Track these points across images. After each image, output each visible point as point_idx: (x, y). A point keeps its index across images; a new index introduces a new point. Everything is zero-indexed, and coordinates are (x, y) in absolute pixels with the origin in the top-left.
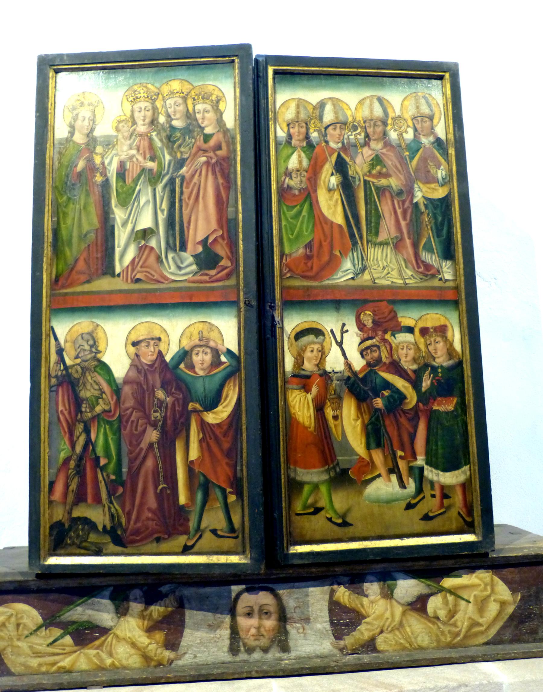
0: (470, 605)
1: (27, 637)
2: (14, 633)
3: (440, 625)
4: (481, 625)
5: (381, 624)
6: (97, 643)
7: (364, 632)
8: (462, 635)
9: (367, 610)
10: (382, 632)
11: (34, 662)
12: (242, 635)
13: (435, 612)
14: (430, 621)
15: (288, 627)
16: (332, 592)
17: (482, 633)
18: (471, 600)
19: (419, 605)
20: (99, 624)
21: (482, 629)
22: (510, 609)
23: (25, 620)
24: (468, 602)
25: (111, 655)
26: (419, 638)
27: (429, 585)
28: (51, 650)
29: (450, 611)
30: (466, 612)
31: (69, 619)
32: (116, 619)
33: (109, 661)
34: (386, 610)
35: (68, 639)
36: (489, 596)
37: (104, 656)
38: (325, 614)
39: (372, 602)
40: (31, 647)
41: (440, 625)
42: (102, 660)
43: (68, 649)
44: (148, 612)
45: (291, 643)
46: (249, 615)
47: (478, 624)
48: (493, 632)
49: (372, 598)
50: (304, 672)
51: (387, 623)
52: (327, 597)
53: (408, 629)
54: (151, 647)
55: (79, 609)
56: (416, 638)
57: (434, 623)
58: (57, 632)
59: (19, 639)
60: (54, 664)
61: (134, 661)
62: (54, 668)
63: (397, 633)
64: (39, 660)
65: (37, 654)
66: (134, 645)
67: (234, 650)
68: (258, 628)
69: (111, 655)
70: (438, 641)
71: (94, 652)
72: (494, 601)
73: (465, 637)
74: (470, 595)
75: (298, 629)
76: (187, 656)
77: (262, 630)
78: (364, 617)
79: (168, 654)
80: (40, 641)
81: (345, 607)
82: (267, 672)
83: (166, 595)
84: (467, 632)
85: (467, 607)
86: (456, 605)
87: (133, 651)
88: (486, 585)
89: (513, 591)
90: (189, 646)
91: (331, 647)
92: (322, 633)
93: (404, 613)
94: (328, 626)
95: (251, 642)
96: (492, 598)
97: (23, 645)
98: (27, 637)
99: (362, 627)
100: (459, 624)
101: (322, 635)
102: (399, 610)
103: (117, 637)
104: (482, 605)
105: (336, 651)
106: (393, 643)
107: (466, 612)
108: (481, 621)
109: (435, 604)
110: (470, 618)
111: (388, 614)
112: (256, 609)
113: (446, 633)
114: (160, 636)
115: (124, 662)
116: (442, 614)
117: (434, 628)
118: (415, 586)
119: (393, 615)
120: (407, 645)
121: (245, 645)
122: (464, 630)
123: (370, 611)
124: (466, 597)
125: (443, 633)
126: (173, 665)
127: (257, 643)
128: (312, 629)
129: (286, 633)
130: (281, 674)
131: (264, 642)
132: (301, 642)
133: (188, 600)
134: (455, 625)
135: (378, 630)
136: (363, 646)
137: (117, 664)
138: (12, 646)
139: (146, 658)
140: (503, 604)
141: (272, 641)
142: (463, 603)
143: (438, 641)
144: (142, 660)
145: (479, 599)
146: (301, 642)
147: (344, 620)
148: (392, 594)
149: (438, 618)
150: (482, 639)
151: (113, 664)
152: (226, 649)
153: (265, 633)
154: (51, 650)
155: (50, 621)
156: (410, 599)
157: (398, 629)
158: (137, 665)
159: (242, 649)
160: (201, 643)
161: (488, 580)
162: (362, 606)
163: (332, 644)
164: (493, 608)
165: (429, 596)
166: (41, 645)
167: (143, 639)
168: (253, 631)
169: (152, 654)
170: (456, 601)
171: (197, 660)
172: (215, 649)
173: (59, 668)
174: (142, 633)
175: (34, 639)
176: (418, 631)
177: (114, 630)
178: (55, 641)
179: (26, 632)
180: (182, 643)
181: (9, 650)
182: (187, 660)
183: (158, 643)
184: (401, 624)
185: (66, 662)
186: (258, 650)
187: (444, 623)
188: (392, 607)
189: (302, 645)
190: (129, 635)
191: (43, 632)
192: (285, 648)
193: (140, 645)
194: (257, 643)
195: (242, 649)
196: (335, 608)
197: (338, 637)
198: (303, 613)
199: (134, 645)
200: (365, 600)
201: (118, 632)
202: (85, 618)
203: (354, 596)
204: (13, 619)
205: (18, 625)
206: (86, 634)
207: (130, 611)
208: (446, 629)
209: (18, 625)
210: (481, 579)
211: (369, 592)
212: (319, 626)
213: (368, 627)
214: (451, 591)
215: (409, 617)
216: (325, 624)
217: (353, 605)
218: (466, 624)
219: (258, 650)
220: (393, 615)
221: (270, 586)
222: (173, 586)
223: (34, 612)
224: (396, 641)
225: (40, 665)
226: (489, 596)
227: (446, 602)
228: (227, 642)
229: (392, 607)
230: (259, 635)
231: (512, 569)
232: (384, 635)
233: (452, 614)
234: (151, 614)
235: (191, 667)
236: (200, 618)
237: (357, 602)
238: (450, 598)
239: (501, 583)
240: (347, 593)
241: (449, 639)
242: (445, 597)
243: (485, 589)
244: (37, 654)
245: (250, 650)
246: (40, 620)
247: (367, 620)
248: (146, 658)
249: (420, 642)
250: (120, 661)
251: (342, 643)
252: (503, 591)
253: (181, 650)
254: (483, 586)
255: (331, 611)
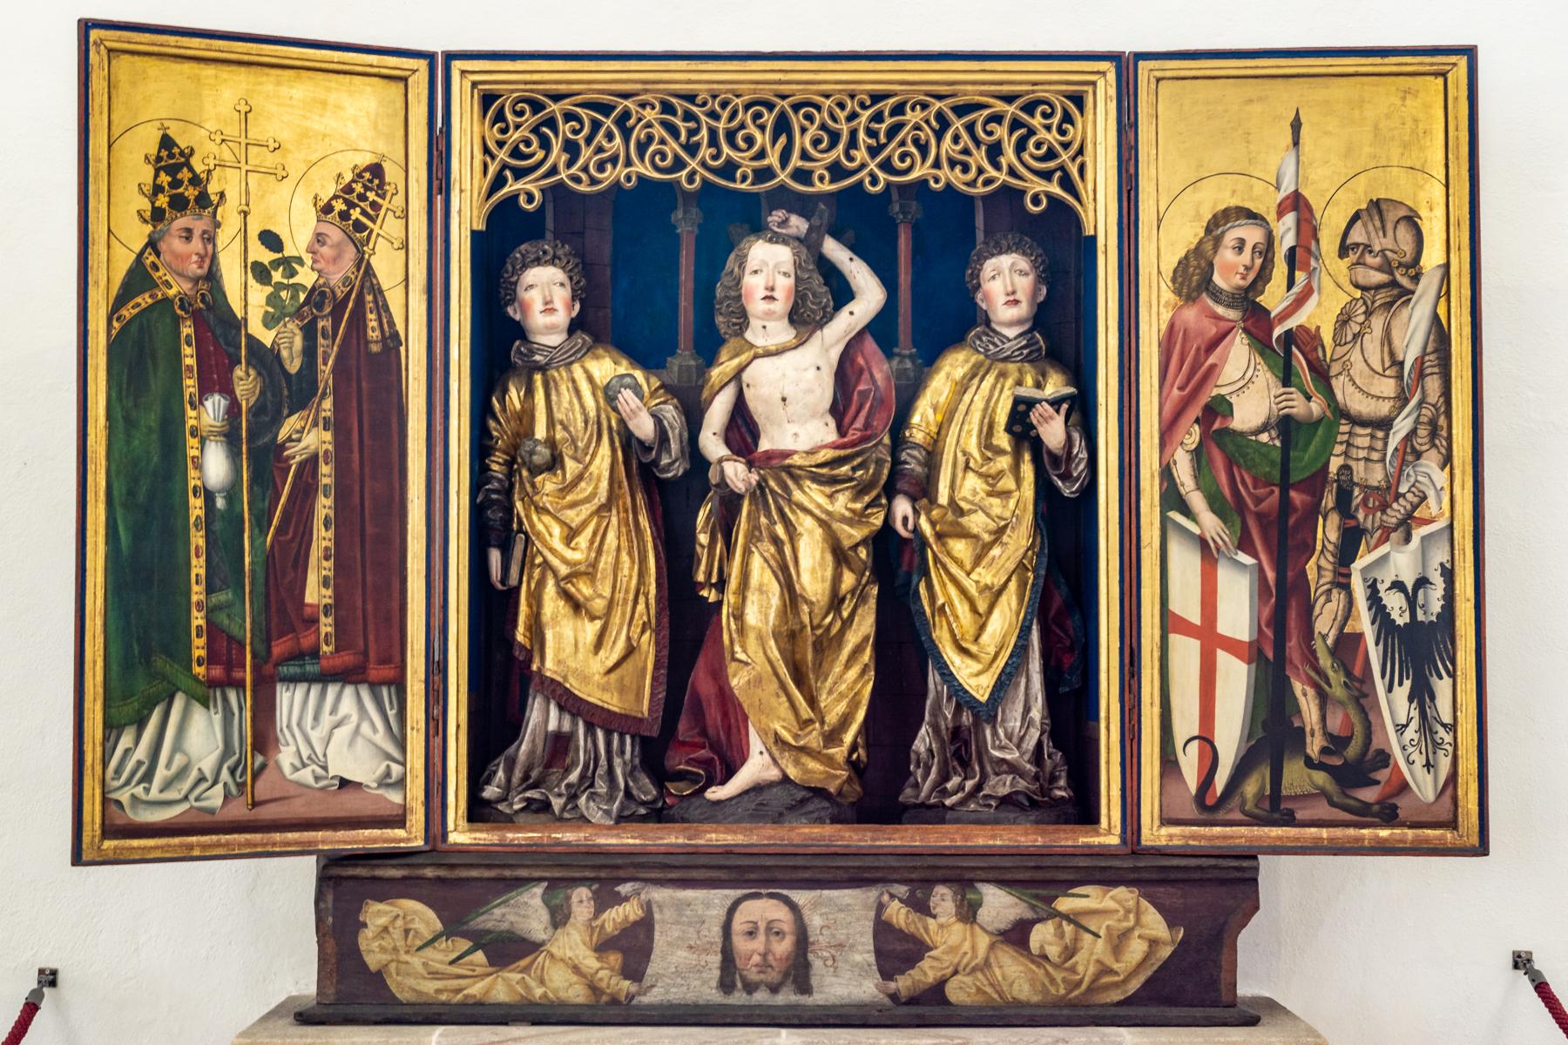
0: (1100, 941)
1: (419, 949)
2: (400, 944)
3: (1049, 968)
4: (1116, 973)
5: (956, 961)
6: (523, 963)
7: (926, 972)
8: (1084, 986)
9: (935, 938)
10: (956, 972)
11: (429, 987)
12: (738, 963)
13: (1042, 947)
14: (1033, 962)
15: (811, 957)
16: (881, 907)
17: (1116, 985)
18: (1102, 933)
19: (1016, 936)
20: (527, 936)
21: (1116, 979)
22: (1166, 952)
23: (417, 925)
24: (1097, 936)
25: (542, 982)
26: (1016, 986)
27: (1033, 907)
28: (454, 970)
29: (1066, 947)
30: (1093, 952)
31: (481, 927)
32: (550, 931)
33: (538, 992)
34: (965, 939)
35: (479, 956)
36: (1130, 930)
37: (533, 984)
38: (867, 941)
39: (941, 926)
40: (425, 964)
41: (1049, 968)
42: (527, 988)
43: (479, 970)
44: (598, 922)
45: (814, 981)
46: (751, 934)
47: (1111, 972)
48: (1135, 985)
49: (942, 920)
50: (831, 1021)
51: (965, 961)
52: (872, 914)
53: (998, 972)
54: (602, 974)
55: (497, 912)
56: (1011, 985)
57: (1039, 965)
58: (464, 945)
59: (407, 952)
60: (459, 991)
61: (576, 993)
62: (459, 997)
63: (980, 975)
64: (439, 984)
65: (435, 975)
66: (576, 969)
67: (726, 985)
68: (764, 956)
69: (542, 982)
70: (1045, 991)
71: (519, 976)
72: (1140, 937)
73: (1089, 990)
74: (1101, 926)
75: (826, 960)
76: (655, 990)
77: (770, 958)
78: (930, 949)
79: (626, 985)
80: (439, 956)
81: (901, 931)
82: (773, 1017)
83: (626, 899)
84: (1094, 981)
85: (1094, 943)
86: (1076, 939)
87: (575, 978)
88: (1128, 911)
89: (1171, 925)
90: (659, 976)
91: (875, 991)
92: (862, 968)
93: (992, 947)
94: (871, 958)
95: (753, 975)
96: (1136, 933)
97: (416, 961)
98: (419, 949)
99: (925, 964)
100: (1080, 969)
101: (862, 970)
102: (983, 942)
103: (552, 956)
104: (1119, 942)
105: (887, 1001)
106: (973, 991)
107: (1093, 952)
108: (1116, 966)
109: (1042, 936)
110: (1098, 961)
111: (967, 946)
112: (762, 926)
113: (1059, 980)
114: (615, 959)
115: (563, 995)
116: (1053, 951)
117: (1040, 972)
118: (1011, 906)
119: (974, 948)
120: (996, 996)
121: (743, 978)
122: (1087, 979)
123: (938, 939)
124: (1093, 928)
125: (1053, 981)
126: (634, 1002)
127: (762, 976)
128: (846, 961)
129: (807, 965)
130: (796, 1021)
131: (773, 976)
132: (829, 980)
133: (660, 907)
134: (1073, 970)
135: (951, 970)
136: (926, 992)
137: (551, 995)
138: (399, 962)
139: (594, 988)
140: (1154, 943)
141: (786, 975)
142: (1088, 937)
143: (1045, 991)
144: (589, 992)
145: (1115, 933)
146: (829, 980)
147: (897, 949)
148: (975, 914)
149: (1045, 957)
150: (1116, 996)
151: (545, 995)
152: (714, 983)
153: (774, 963)
154: (454, 970)
155: (453, 926)
156: (1002, 926)
157: (982, 970)
158: (581, 1000)
159: (739, 985)
160: (678, 973)
161: (1131, 904)
162: (926, 930)
163: (876, 986)
164: (1136, 949)
165: (1033, 923)
166: (442, 962)
167: (590, 962)
168: (756, 959)
169: (603, 985)
170: (1076, 933)
171: (671, 997)
172: (697, 983)
173: (466, 996)
174: (589, 953)
175: (429, 952)
176: (1015, 976)
177: (547, 947)
178: (459, 958)
179: (419, 943)
180: (649, 971)
181: (393, 966)
182: (653, 997)
183: (612, 969)
184: (987, 963)
185: (476, 989)
186: (763, 987)
187: (1056, 966)
188: (973, 935)
189: (831, 985)
190: (569, 954)
191: (442, 944)
192: (805, 988)
193: (584, 969)
194: (762, 976)
195: (739, 985)
196: (883, 929)
197: (887, 974)
198: (833, 936)
199: (576, 969)
200: (930, 921)
201: (554, 950)
202: (505, 926)
203: (914, 916)
204: (399, 922)
205: (407, 931)
206: (508, 949)
207: (572, 920)
208: (1059, 976)
209: (407, 931)
210: (1119, 902)
211: (937, 911)
212: (858, 958)
213: (935, 964)
214: (1066, 917)
215: (1000, 954)
216: (866, 956)
217: (912, 929)
218: (1092, 970)
219: (763, 987)
220: (974, 948)
221: (785, 892)
222: (637, 885)
223: (431, 914)
224: (979, 990)
225: (438, 991)
226: (1130, 930)
227: (1061, 935)
228: (717, 973)
229: (973, 935)
230: (765, 965)
231: (1171, 890)
232: (958, 977)
233: (1070, 952)
234: (602, 927)
235: (660, 1006)
236: (676, 934)
237: (920, 926)
238: (1068, 929)
239: (1152, 909)
240: (904, 911)
241: (1062, 991)
242: (1060, 925)
243: (1126, 918)
244: (435, 975)
245: (750, 988)
246: (439, 926)
247: (931, 953)
248: (594, 988)
249: (1016, 993)
250: (555, 991)
251: (892, 985)
252: (1155, 923)
253: (647, 981)
254: (1122, 912)
255: (877, 935)
